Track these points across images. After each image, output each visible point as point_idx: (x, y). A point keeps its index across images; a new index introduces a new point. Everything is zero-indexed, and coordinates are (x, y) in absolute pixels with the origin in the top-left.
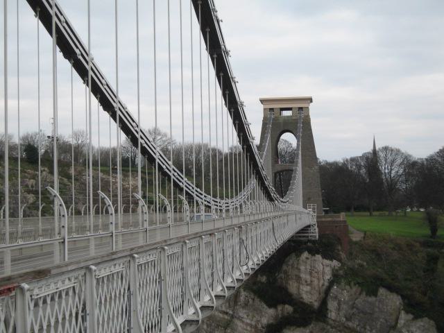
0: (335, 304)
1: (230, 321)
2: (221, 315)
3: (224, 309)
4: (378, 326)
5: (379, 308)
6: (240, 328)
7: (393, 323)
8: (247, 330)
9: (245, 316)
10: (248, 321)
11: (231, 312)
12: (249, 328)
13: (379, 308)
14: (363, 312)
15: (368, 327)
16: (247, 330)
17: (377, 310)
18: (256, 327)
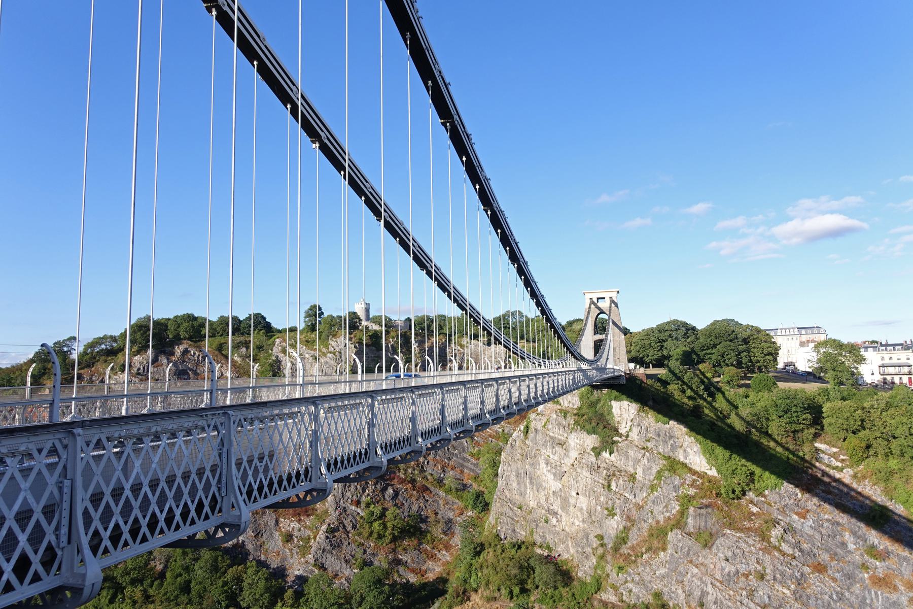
4: (669, 446)
10: (578, 442)
13: (669, 433)
17: (668, 434)
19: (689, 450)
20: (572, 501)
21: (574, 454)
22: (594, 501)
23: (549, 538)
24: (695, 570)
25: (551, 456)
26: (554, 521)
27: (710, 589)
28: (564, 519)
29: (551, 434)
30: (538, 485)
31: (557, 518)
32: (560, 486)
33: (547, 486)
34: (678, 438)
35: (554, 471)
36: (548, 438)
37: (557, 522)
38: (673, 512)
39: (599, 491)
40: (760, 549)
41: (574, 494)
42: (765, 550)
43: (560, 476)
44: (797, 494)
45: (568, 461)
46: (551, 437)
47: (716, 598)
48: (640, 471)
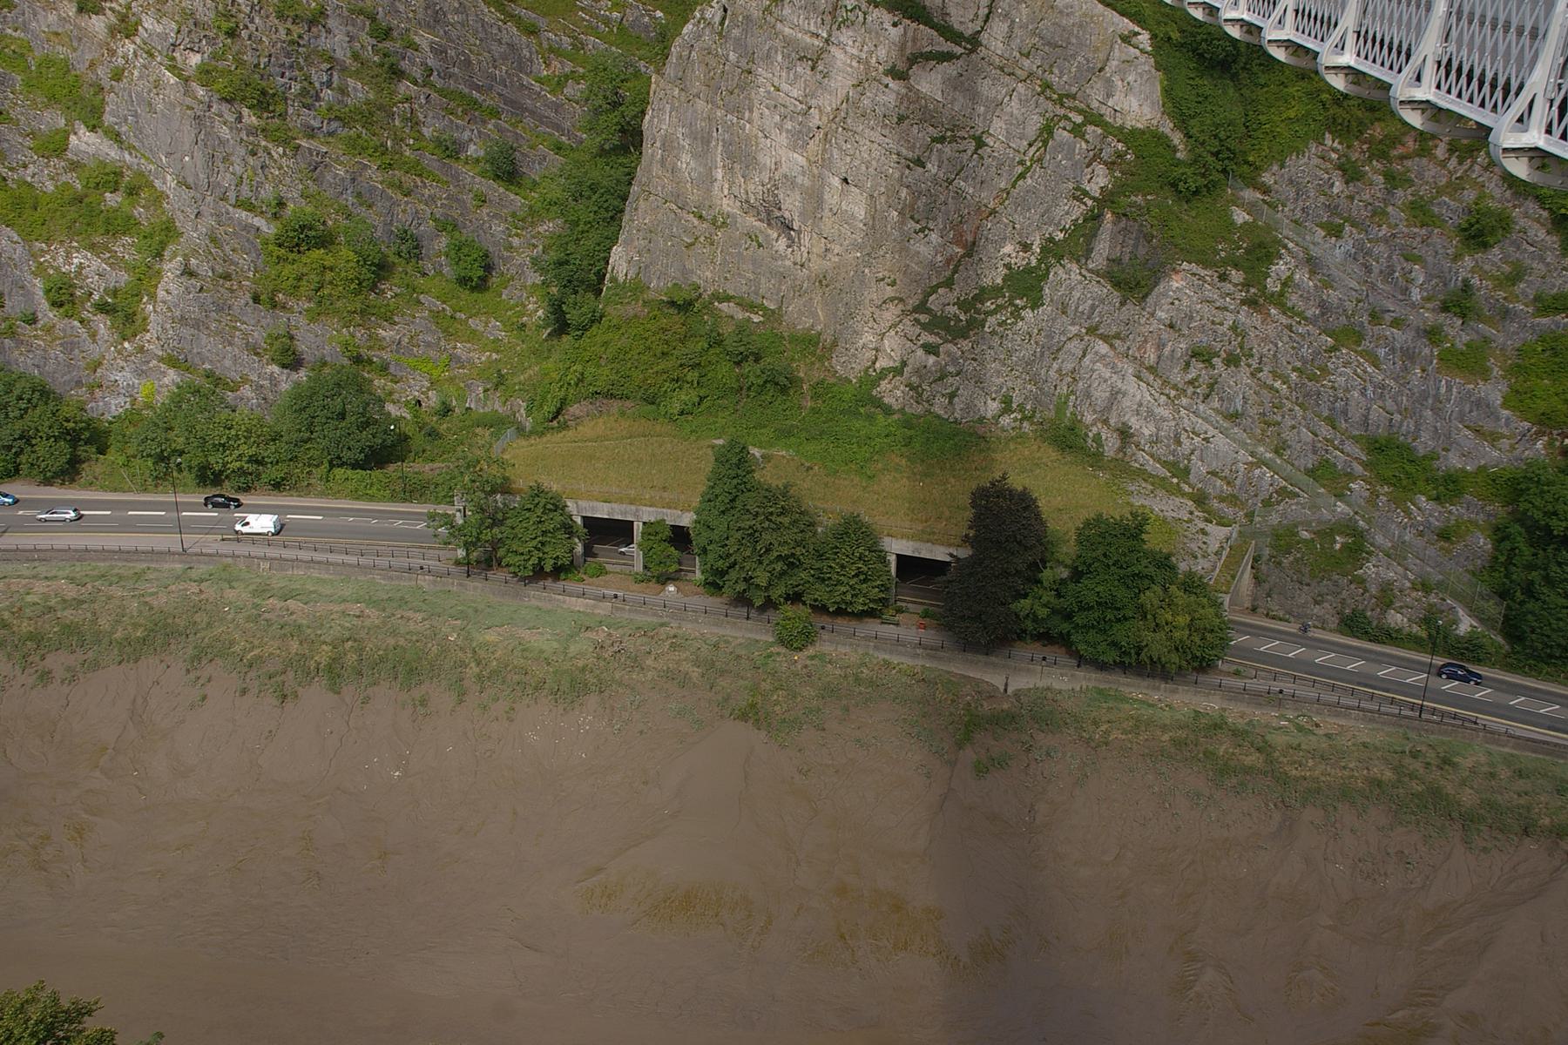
0: (1005, 26)
1: (823, 50)
2: (808, 39)
3: (812, 28)
5: (1077, 37)
6: (838, 62)
7: (1099, 66)
8: (851, 67)
9: (851, 43)
10: (855, 52)
11: (825, 35)
12: (855, 64)
13: (1077, 37)
14: (1049, 44)
15: (1056, 71)
16: (851, 67)
17: (1074, 41)
18: (867, 62)
19: (1116, 79)
20: (831, 198)
21: (841, 83)
22: (883, 199)
23: (765, 285)
24: (1103, 348)
25: (785, 87)
26: (783, 242)
27: (1131, 386)
28: (806, 240)
29: (787, 31)
30: (742, 156)
31: (790, 238)
32: (801, 160)
33: (767, 160)
34: (1097, 49)
35: (789, 125)
36: (778, 43)
37: (789, 246)
38: (1063, 222)
39: (897, 175)
40: (1243, 302)
41: (836, 182)
42: (1251, 303)
43: (800, 139)
44: (1332, 185)
45: (828, 102)
46: (788, 42)
47: (1140, 405)
48: (998, 127)
